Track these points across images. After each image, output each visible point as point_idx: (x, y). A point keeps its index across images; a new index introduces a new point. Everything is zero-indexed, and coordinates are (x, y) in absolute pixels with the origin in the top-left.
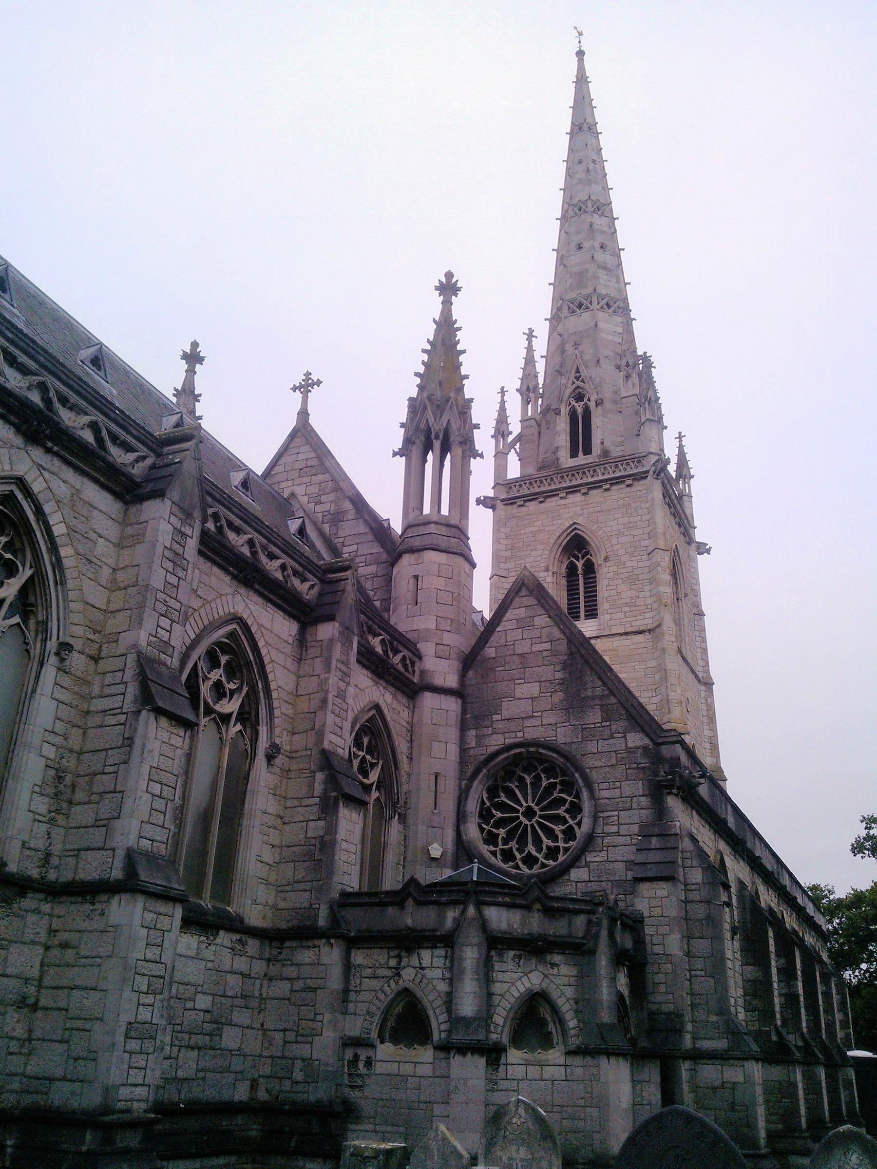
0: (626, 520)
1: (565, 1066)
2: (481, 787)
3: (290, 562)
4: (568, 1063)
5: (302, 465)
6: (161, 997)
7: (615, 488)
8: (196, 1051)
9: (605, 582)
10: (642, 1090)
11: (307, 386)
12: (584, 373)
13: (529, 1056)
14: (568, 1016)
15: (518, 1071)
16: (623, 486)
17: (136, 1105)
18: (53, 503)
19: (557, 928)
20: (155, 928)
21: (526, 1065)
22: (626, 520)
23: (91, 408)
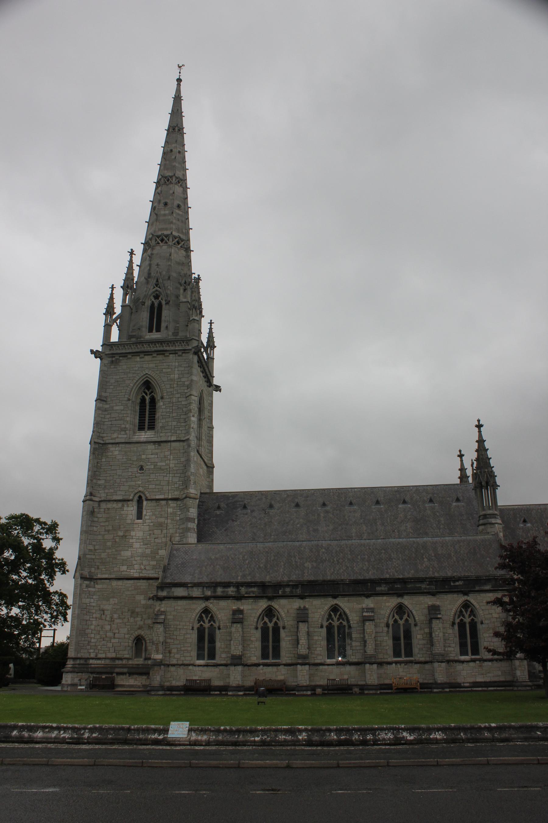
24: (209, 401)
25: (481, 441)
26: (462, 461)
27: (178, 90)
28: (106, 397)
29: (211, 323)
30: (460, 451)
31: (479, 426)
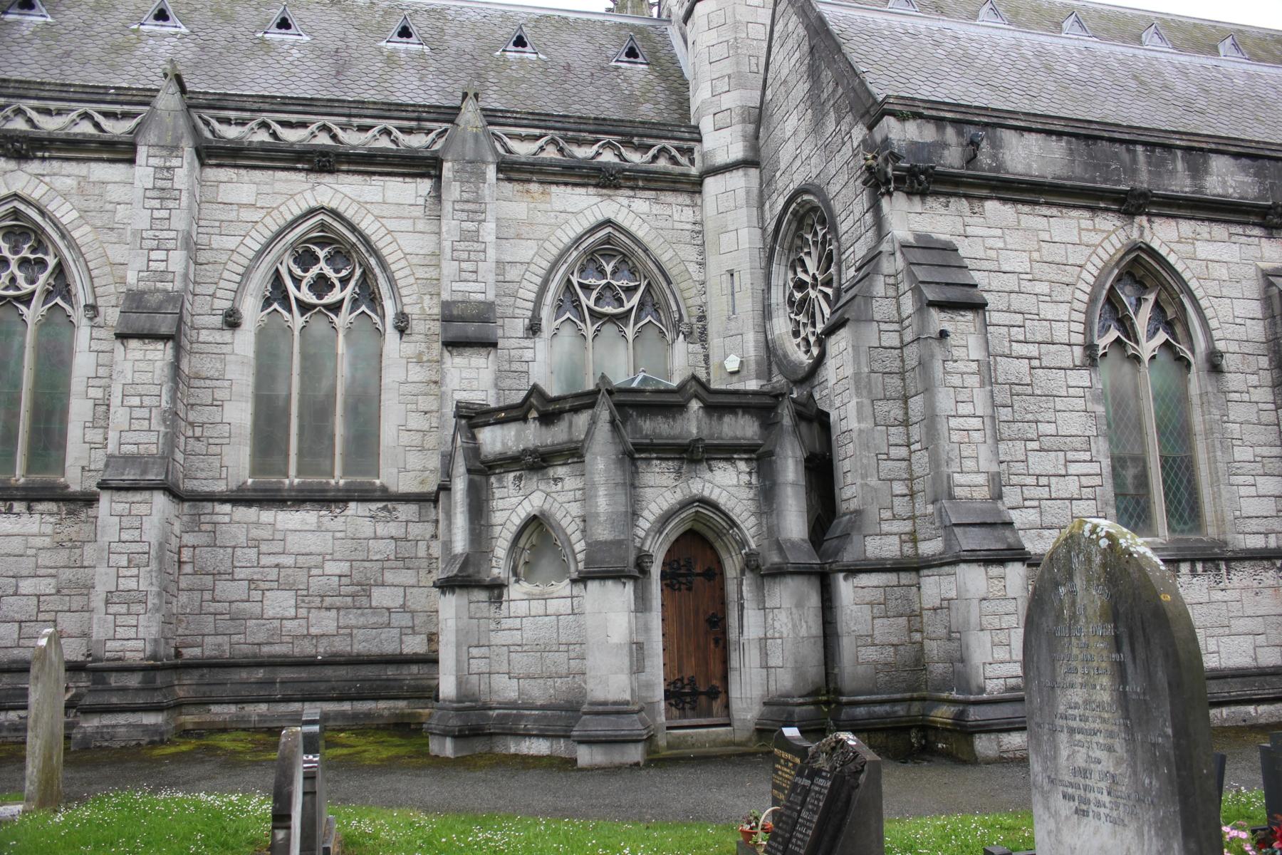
1: (572, 597)
2: (783, 268)
3: (390, 124)
4: (575, 593)
6: (148, 569)
8: (334, 612)
10: (773, 620)
13: (536, 590)
14: (574, 538)
15: (520, 608)
17: (128, 654)
18: (59, 200)
19: (556, 435)
20: (130, 515)
21: (529, 600)
23: (73, 104)
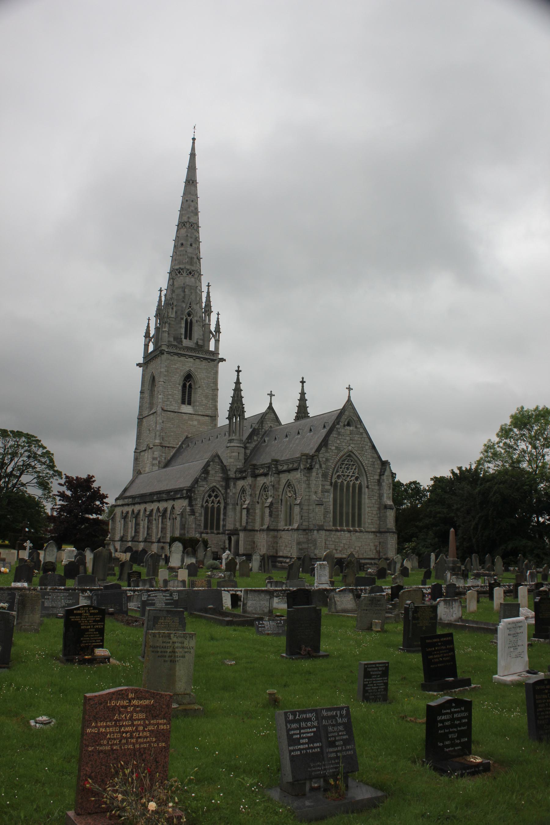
0: (206, 374)
5: (272, 418)
7: (204, 361)
9: (198, 395)
11: (271, 395)
12: (194, 306)
16: (206, 361)
22: (206, 374)
24: (214, 371)
25: (238, 383)
26: (303, 386)
27: (193, 148)
28: (144, 390)
29: (218, 314)
30: (303, 378)
31: (238, 371)
